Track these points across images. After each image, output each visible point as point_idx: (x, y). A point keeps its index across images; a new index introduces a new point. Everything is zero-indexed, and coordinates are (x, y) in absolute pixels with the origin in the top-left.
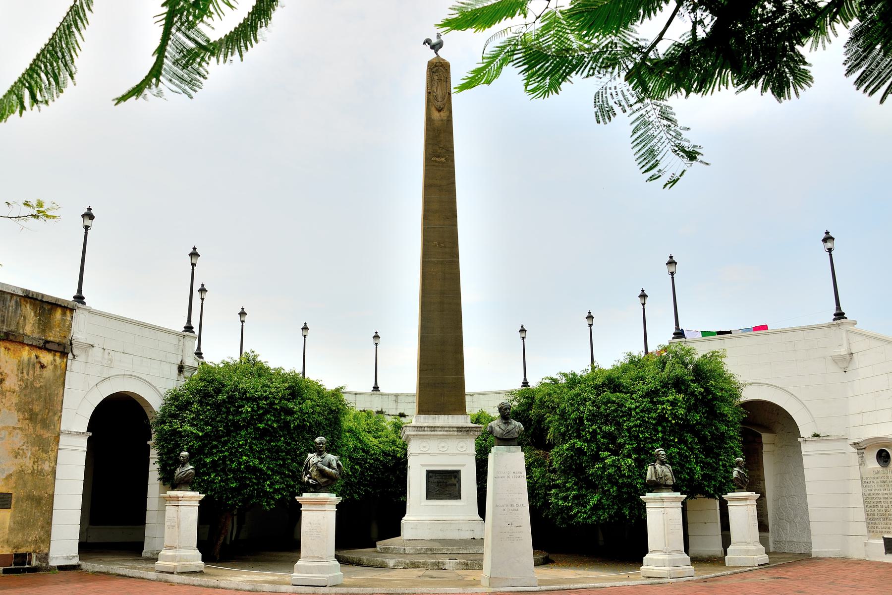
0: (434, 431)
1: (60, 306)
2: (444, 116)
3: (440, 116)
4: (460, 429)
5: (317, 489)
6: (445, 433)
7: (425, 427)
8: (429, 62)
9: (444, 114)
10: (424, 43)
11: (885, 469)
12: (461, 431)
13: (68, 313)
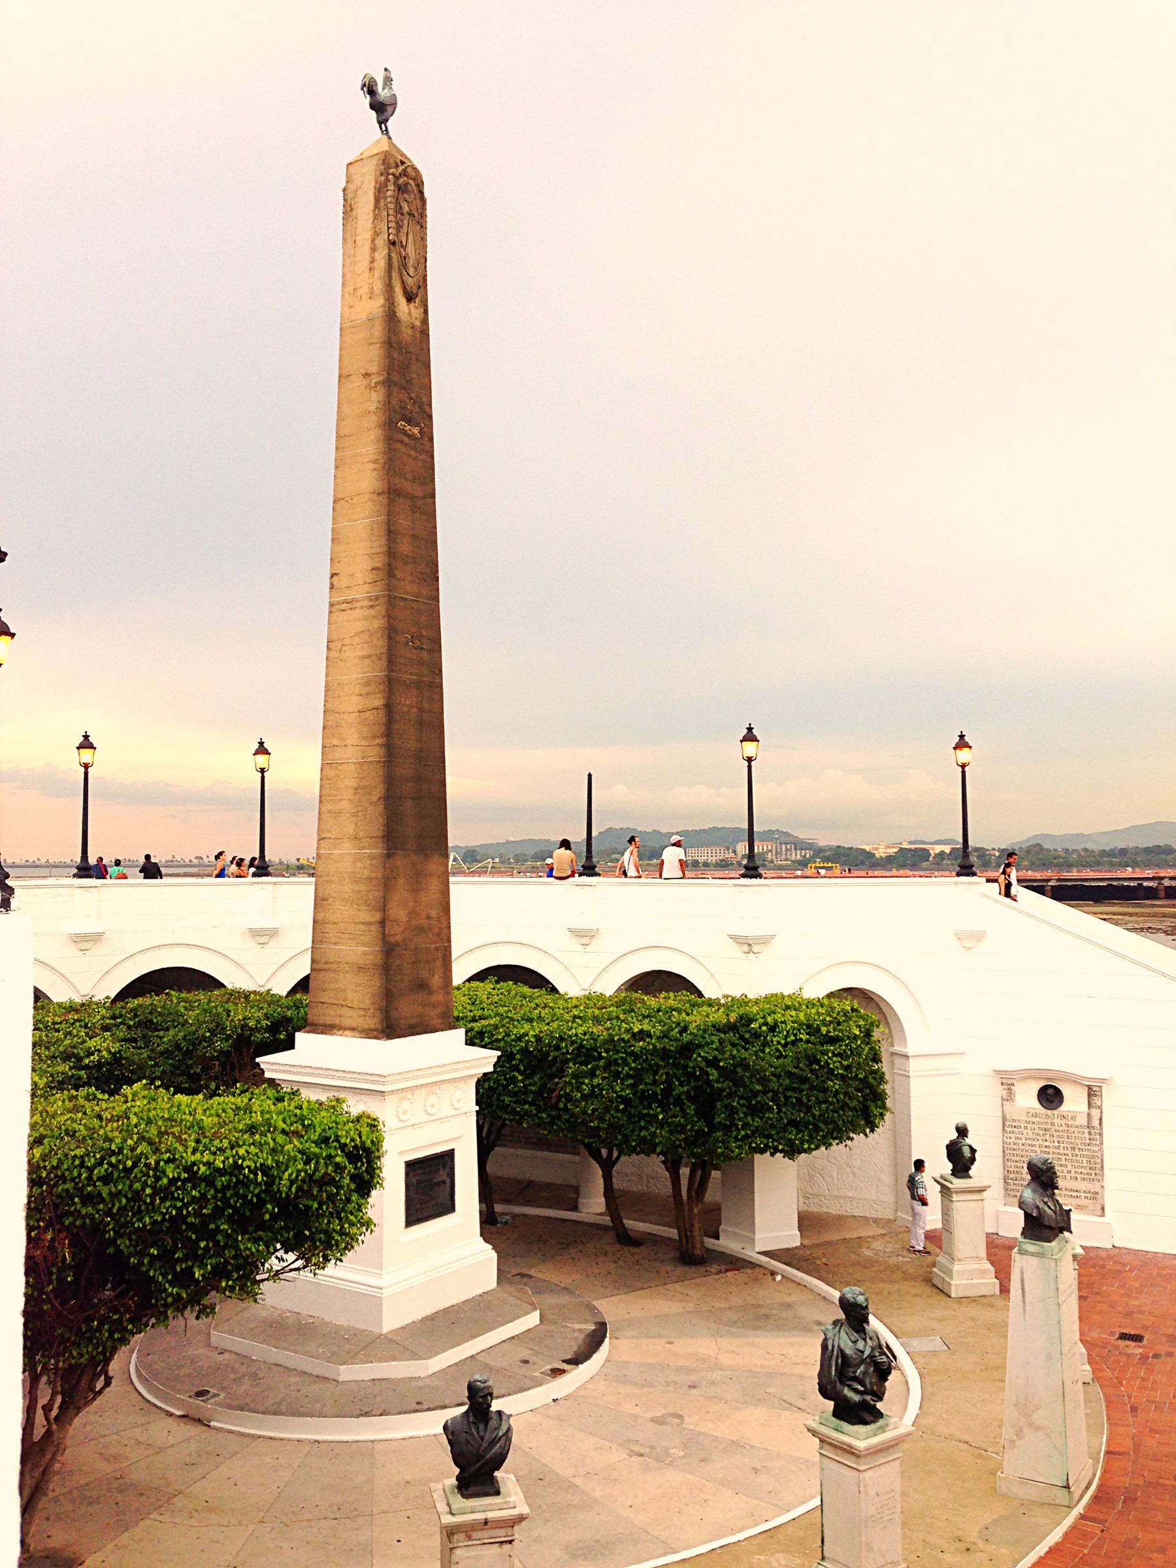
2: (416, 318)
3: (410, 314)
11: (1049, 1112)
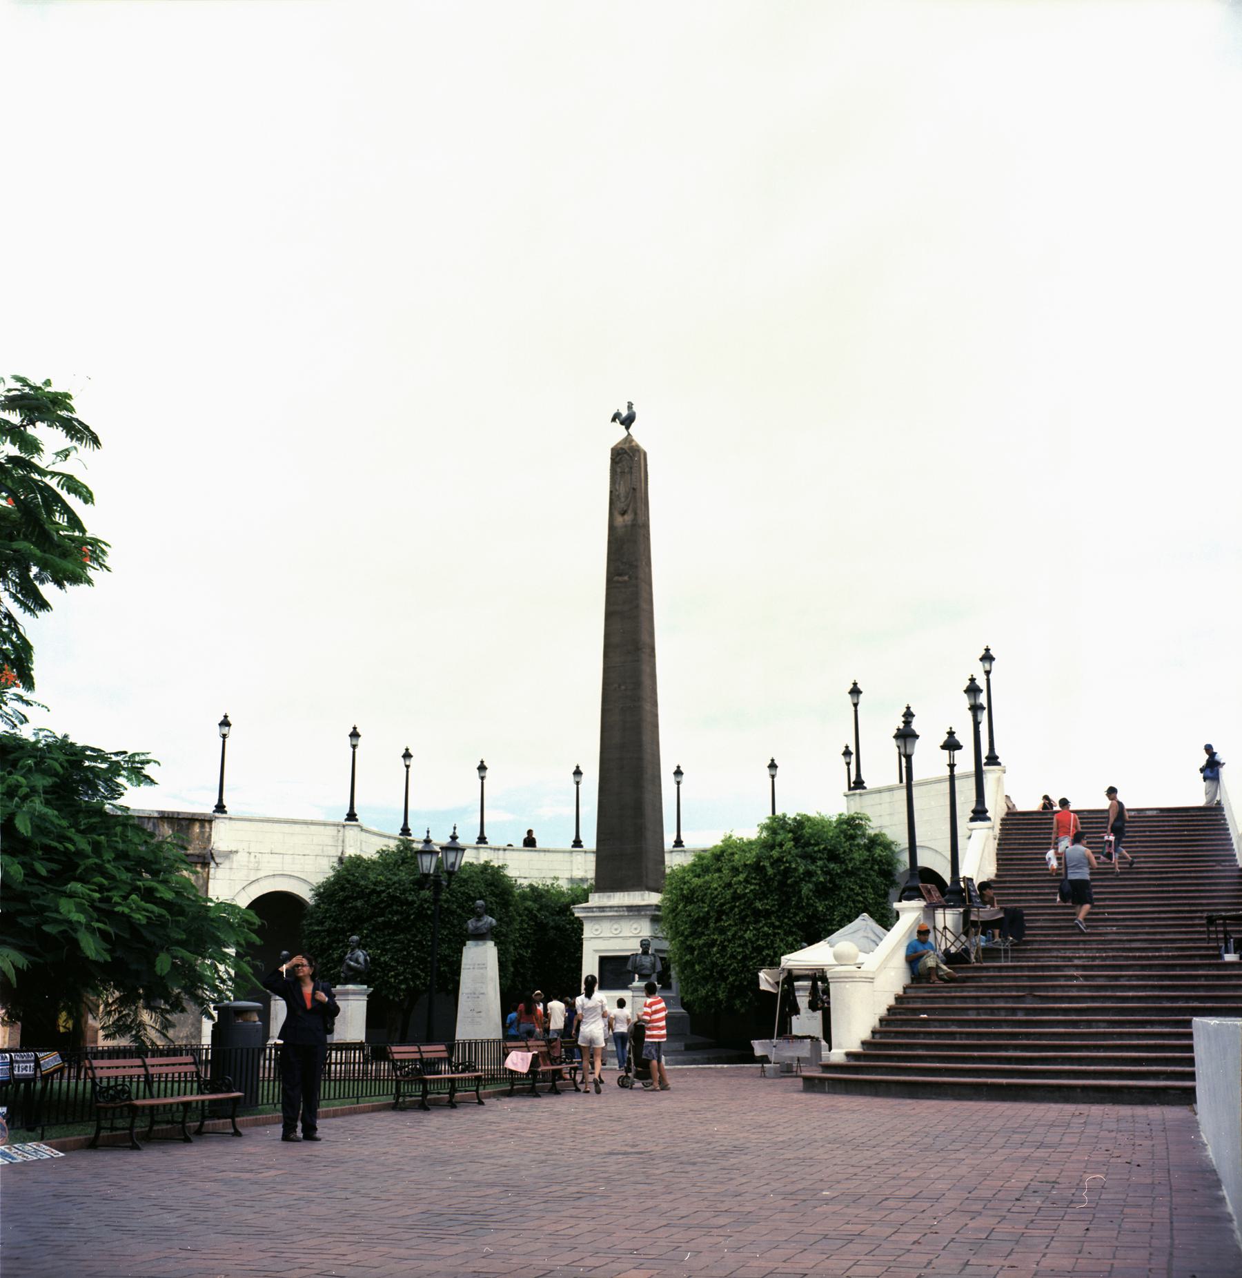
0: (604, 911)
1: (197, 820)
3: (624, 521)
4: (630, 908)
5: (347, 981)
6: (615, 914)
7: (593, 908)
8: (612, 449)
9: (628, 518)
10: (614, 420)
12: (631, 911)
13: (207, 825)
